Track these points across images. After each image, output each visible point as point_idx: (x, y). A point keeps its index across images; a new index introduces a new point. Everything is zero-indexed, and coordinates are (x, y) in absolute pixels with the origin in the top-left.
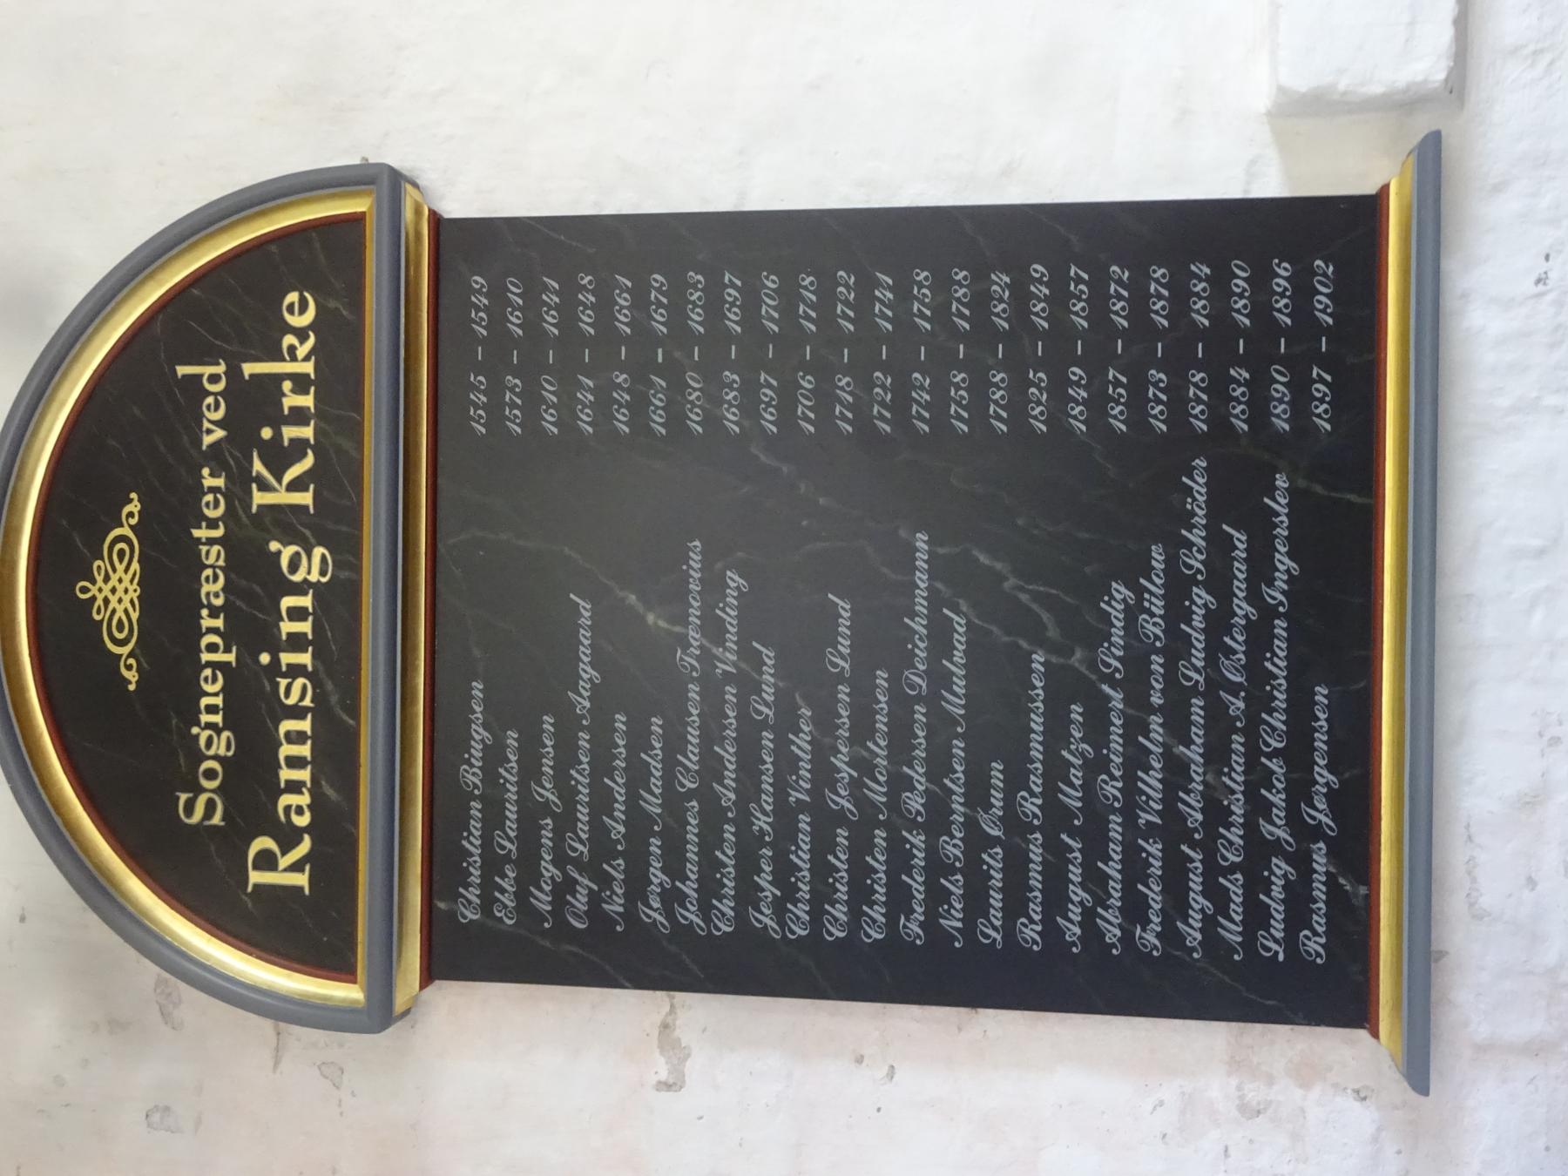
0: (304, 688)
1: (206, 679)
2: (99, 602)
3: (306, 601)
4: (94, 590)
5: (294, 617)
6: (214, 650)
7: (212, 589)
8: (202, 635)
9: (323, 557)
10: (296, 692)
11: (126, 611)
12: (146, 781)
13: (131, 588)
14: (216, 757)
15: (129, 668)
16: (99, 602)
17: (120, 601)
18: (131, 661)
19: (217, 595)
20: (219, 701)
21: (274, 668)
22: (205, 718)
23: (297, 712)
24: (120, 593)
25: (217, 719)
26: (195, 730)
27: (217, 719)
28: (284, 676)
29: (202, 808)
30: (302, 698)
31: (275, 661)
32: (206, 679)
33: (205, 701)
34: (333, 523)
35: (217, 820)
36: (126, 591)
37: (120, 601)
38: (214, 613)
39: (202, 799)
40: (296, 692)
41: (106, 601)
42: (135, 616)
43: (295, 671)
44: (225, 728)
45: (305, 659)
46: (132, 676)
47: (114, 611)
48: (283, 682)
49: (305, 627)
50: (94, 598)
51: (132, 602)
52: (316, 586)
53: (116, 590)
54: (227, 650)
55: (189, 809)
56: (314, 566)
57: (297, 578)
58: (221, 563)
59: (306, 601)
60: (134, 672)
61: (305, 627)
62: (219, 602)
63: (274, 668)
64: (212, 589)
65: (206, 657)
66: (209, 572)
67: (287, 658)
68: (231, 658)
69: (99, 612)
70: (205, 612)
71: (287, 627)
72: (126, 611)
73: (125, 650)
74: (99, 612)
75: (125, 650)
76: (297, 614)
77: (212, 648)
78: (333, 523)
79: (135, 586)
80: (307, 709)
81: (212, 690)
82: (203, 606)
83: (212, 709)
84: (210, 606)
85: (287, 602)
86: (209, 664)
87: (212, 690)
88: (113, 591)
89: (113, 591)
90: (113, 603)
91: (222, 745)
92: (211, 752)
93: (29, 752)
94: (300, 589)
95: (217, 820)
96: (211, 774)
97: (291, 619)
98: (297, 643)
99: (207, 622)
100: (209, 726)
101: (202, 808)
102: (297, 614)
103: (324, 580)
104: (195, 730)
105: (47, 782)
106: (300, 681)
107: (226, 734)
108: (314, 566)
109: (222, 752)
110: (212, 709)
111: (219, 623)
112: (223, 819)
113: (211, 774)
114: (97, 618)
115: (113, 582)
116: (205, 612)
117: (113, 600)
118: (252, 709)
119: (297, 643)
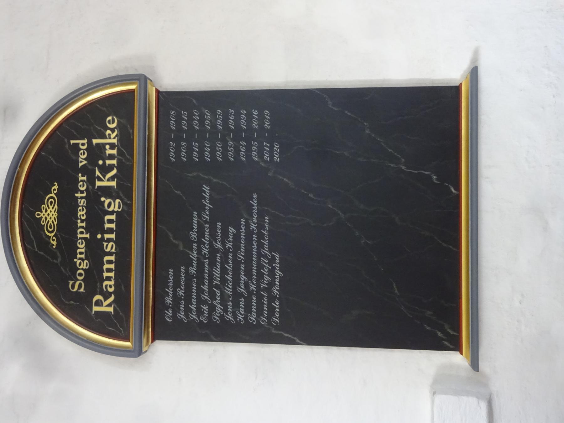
0: (112, 246)
1: (79, 243)
2: (44, 219)
3: (113, 217)
4: (42, 215)
5: (110, 222)
6: (82, 235)
7: (82, 213)
8: (78, 229)
9: (119, 202)
10: (110, 247)
11: (53, 221)
12: (60, 276)
13: (54, 214)
14: (82, 269)
15: (53, 240)
16: (44, 219)
17: (51, 218)
18: (54, 238)
19: (83, 215)
20: (83, 250)
21: (103, 239)
22: (79, 256)
23: (110, 254)
24: (51, 215)
25: (83, 256)
26: (75, 260)
27: (83, 256)
28: (106, 242)
29: (78, 286)
30: (112, 248)
31: (103, 237)
32: (79, 243)
33: (79, 251)
34: (124, 190)
35: (82, 290)
36: (53, 215)
37: (51, 218)
38: (82, 221)
39: (78, 283)
40: (110, 247)
41: (46, 218)
42: (55, 223)
43: (109, 240)
44: (86, 259)
45: (113, 236)
46: (54, 243)
47: (48, 221)
48: (105, 244)
49: (113, 226)
50: (42, 217)
51: (55, 218)
52: (117, 212)
53: (49, 214)
54: (87, 234)
55: (73, 287)
56: (116, 206)
57: (111, 209)
58: (85, 205)
59: (113, 217)
60: (55, 242)
61: (113, 226)
62: (83, 218)
63: (103, 239)
64: (82, 213)
65: (79, 236)
66: (80, 208)
67: (107, 236)
68: (88, 236)
69: (43, 222)
70: (79, 221)
71: (107, 226)
72: (53, 221)
73: (52, 235)
74: (43, 222)
75: (52, 235)
76: (110, 221)
77: (82, 233)
78: (124, 190)
79: (56, 213)
80: (113, 253)
81: (81, 247)
82: (78, 219)
83: (81, 253)
84: (81, 219)
85: (107, 217)
86: (80, 238)
87: (81, 247)
88: (48, 215)
89: (48, 215)
90: (48, 219)
91: (85, 265)
92: (81, 267)
93: (12, 237)
94: (112, 213)
95: (82, 290)
96: (80, 275)
97: (108, 223)
98: (110, 231)
99: (80, 224)
100: (80, 259)
101: (78, 286)
102: (110, 221)
103: (120, 210)
104: (75, 260)
105: (13, 219)
106: (111, 244)
107: (86, 261)
108: (116, 206)
109: (84, 267)
110: (81, 253)
111: (84, 224)
112: (84, 290)
113: (80, 275)
114: (43, 224)
115: (49, 211)
116: (79, 221)
117: (48, 218)
118: (95, 251)
119: (110, 231)
